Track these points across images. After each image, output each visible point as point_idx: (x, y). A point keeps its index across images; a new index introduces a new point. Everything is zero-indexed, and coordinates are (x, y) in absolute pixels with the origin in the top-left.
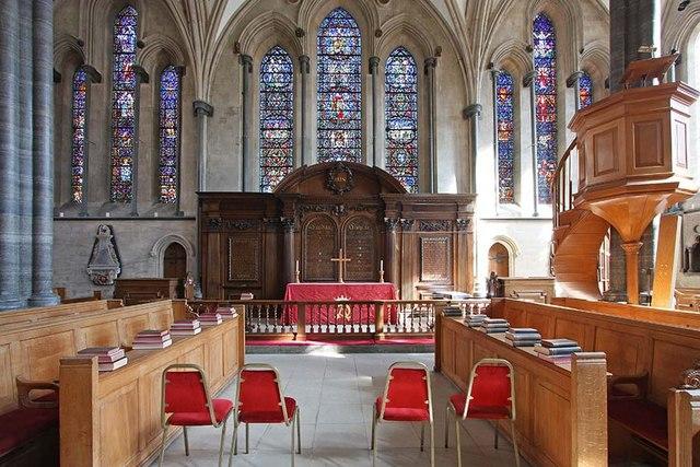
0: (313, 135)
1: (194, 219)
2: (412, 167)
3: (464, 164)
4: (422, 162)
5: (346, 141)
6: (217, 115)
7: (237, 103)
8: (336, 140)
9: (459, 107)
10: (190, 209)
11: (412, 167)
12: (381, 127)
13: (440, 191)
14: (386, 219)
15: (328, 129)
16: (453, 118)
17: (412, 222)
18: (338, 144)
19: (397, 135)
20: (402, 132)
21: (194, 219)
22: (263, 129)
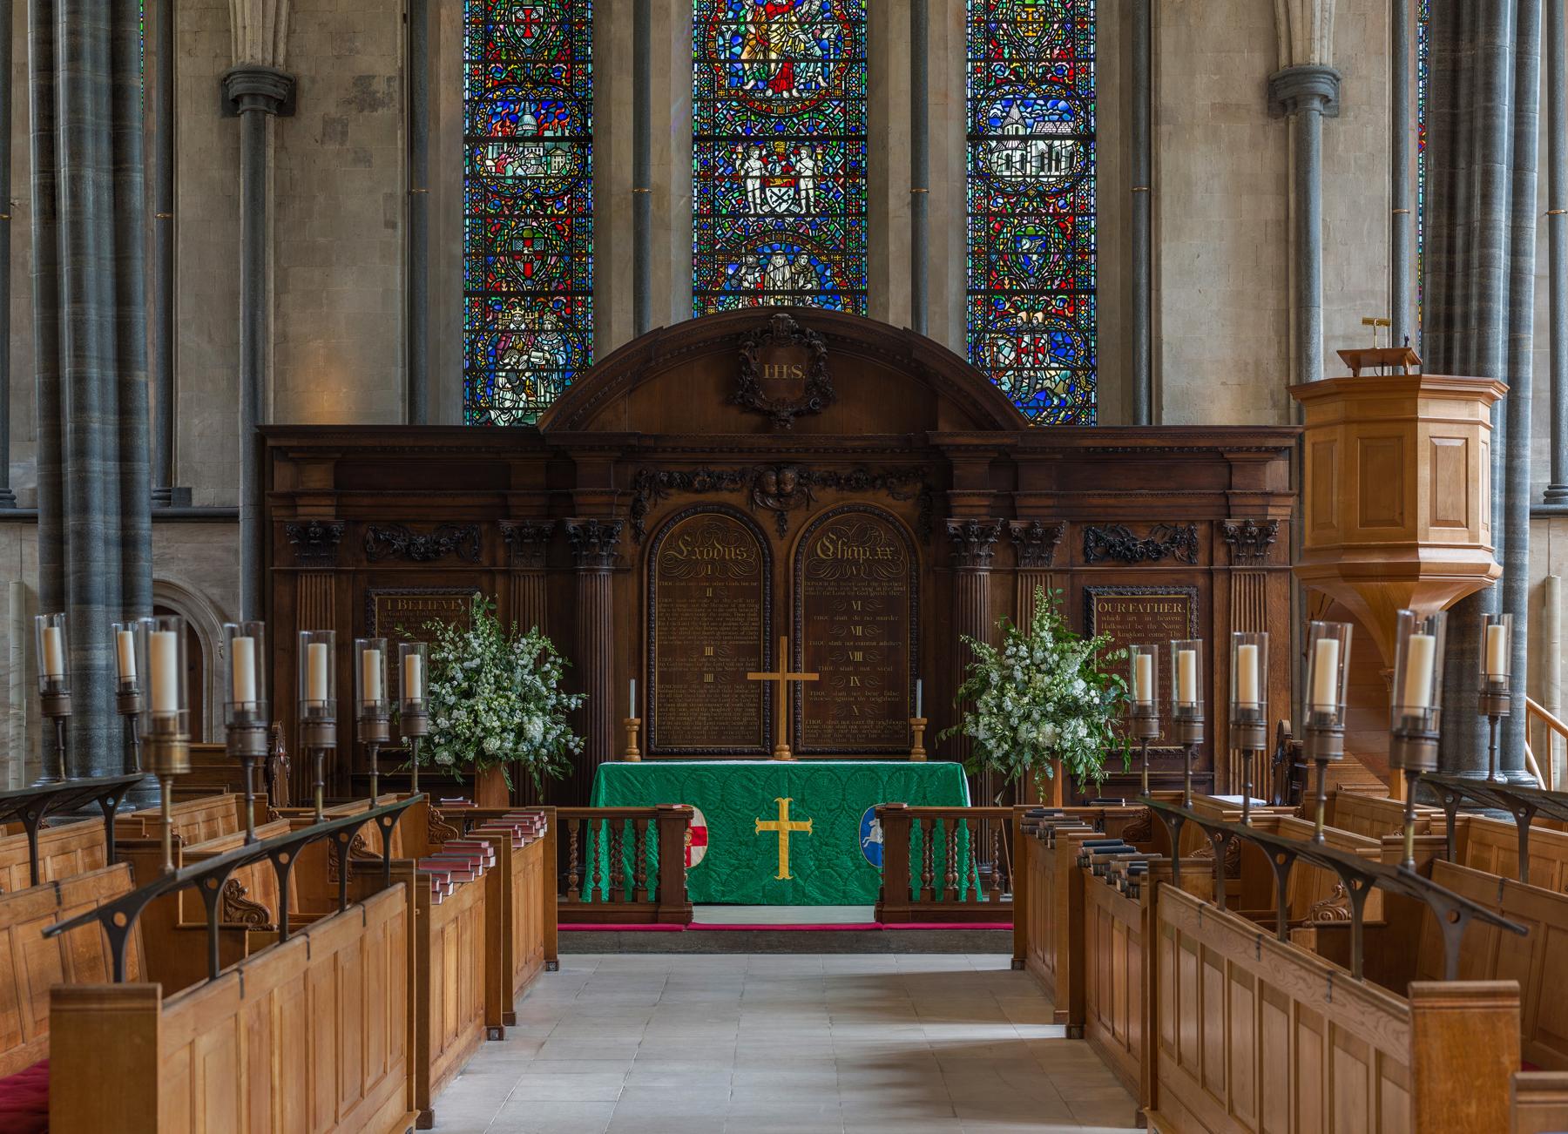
0: (674, 169)
1: (230, 518)
2: (1073, 293)
3: (1271, 299)
4: (1107, 271)
5: (802, 184)
6: (318, 107)
7: (382, 60)
8: (765, 182)
9: (1250, 67)
10: (216, 467)
11: (1073, 293)
12: (947, 133)
13: (1168, 419)
14: (953, 524)
15: (735, 139)
16: (1224, 109)
17: (1051, 534)
18: (778, 199)
19: (1017, 160)
20: (1031, 150)
21: (230, 518)
22: (476, 141)
